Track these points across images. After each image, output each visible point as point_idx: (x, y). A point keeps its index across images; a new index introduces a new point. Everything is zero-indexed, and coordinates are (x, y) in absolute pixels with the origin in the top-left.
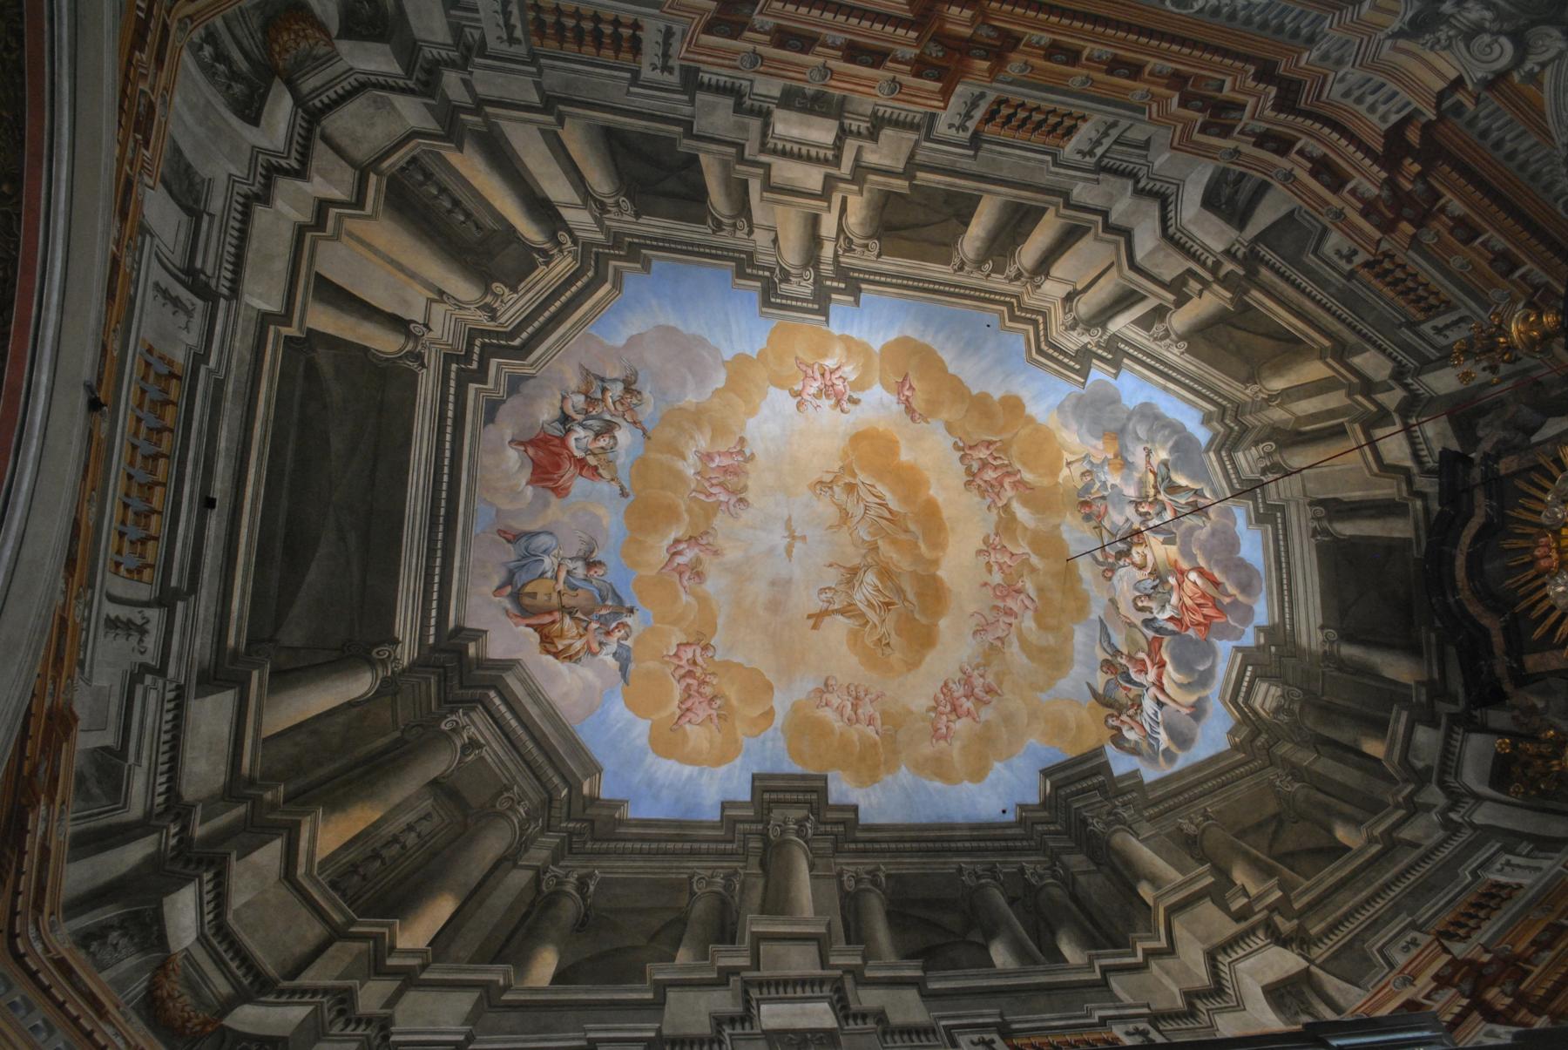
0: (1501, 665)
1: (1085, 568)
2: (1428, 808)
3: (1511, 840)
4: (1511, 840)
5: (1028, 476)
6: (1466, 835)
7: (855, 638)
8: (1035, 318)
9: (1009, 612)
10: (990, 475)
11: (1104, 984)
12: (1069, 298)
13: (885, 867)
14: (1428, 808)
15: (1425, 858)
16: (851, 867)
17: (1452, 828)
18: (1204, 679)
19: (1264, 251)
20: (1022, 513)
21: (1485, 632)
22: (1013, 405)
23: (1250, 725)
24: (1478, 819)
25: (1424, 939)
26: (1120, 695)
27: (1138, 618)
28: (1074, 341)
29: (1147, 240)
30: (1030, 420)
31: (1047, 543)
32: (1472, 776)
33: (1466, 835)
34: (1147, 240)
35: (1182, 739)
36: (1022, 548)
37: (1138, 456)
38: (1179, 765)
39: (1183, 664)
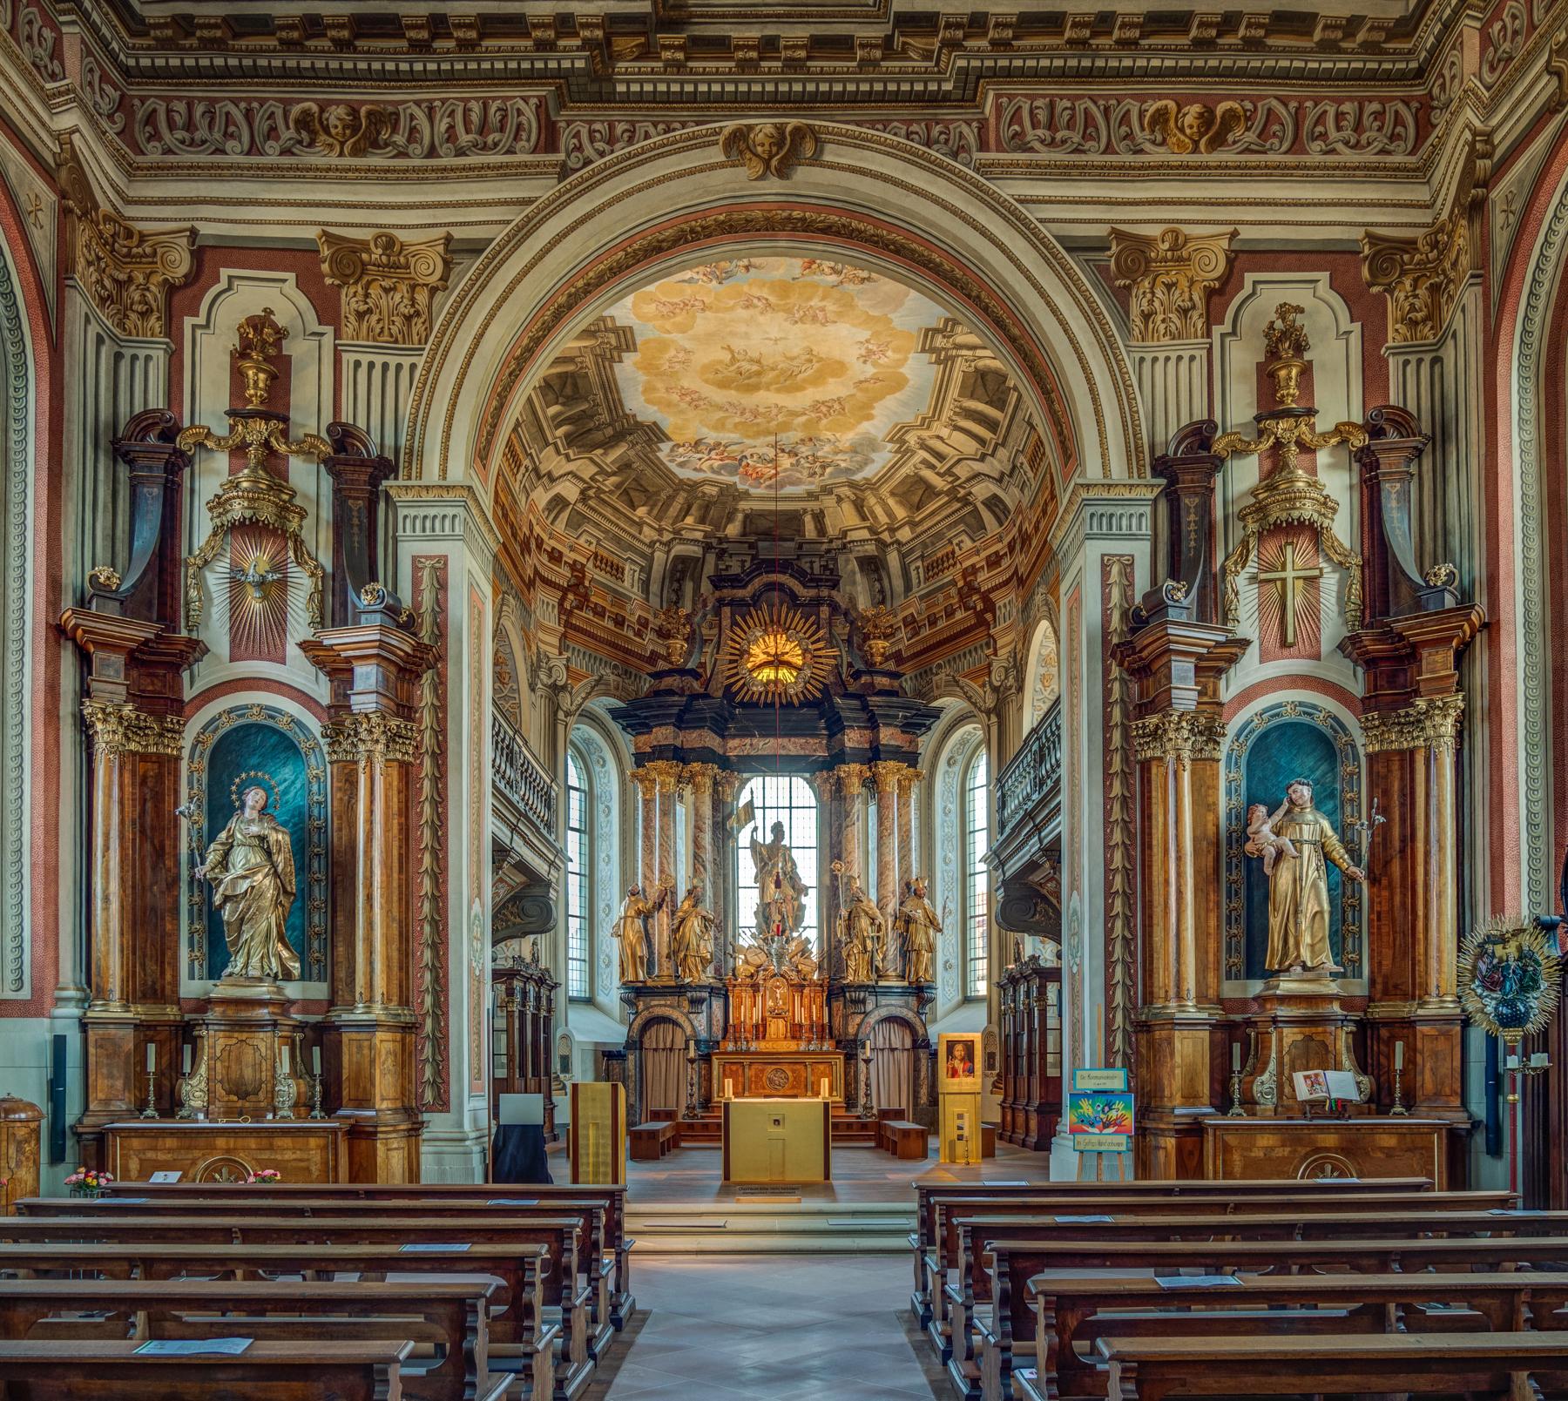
0: (727, 593)
1: (771, 439)
2: (661, 535)
3: (647, 570)
4: (647, 570)
5: (824, 421)
6: (648, 551)
7: (721, 362)
8: (926, 423)
9: (742, 414)
10: (824, 409)
11: (547, 444)
12: (939, 437)
13: (592, 372)
14: (661, 535)
15: (634, 537)
16: (589, 360)
17: (652, 544)
18: (714, 471)
19: (970, 508)
20: (803, 418)
21: (744, 587)
22: (869, 417)
23: (693, 487)
24: (657, 554)
25: (592, 547)
26: (702, 447)
27: (747, 453)
28: (912, 439)
29: (978, 467)
30: (859, 423)
31: (785, 427)
32: (678, 549)
33: (648, 551)
34: (978, 467)
35: (681, 465)
36: (780, 418)
37: (840, 457)
38: (670, 465)
39: (723, 467)
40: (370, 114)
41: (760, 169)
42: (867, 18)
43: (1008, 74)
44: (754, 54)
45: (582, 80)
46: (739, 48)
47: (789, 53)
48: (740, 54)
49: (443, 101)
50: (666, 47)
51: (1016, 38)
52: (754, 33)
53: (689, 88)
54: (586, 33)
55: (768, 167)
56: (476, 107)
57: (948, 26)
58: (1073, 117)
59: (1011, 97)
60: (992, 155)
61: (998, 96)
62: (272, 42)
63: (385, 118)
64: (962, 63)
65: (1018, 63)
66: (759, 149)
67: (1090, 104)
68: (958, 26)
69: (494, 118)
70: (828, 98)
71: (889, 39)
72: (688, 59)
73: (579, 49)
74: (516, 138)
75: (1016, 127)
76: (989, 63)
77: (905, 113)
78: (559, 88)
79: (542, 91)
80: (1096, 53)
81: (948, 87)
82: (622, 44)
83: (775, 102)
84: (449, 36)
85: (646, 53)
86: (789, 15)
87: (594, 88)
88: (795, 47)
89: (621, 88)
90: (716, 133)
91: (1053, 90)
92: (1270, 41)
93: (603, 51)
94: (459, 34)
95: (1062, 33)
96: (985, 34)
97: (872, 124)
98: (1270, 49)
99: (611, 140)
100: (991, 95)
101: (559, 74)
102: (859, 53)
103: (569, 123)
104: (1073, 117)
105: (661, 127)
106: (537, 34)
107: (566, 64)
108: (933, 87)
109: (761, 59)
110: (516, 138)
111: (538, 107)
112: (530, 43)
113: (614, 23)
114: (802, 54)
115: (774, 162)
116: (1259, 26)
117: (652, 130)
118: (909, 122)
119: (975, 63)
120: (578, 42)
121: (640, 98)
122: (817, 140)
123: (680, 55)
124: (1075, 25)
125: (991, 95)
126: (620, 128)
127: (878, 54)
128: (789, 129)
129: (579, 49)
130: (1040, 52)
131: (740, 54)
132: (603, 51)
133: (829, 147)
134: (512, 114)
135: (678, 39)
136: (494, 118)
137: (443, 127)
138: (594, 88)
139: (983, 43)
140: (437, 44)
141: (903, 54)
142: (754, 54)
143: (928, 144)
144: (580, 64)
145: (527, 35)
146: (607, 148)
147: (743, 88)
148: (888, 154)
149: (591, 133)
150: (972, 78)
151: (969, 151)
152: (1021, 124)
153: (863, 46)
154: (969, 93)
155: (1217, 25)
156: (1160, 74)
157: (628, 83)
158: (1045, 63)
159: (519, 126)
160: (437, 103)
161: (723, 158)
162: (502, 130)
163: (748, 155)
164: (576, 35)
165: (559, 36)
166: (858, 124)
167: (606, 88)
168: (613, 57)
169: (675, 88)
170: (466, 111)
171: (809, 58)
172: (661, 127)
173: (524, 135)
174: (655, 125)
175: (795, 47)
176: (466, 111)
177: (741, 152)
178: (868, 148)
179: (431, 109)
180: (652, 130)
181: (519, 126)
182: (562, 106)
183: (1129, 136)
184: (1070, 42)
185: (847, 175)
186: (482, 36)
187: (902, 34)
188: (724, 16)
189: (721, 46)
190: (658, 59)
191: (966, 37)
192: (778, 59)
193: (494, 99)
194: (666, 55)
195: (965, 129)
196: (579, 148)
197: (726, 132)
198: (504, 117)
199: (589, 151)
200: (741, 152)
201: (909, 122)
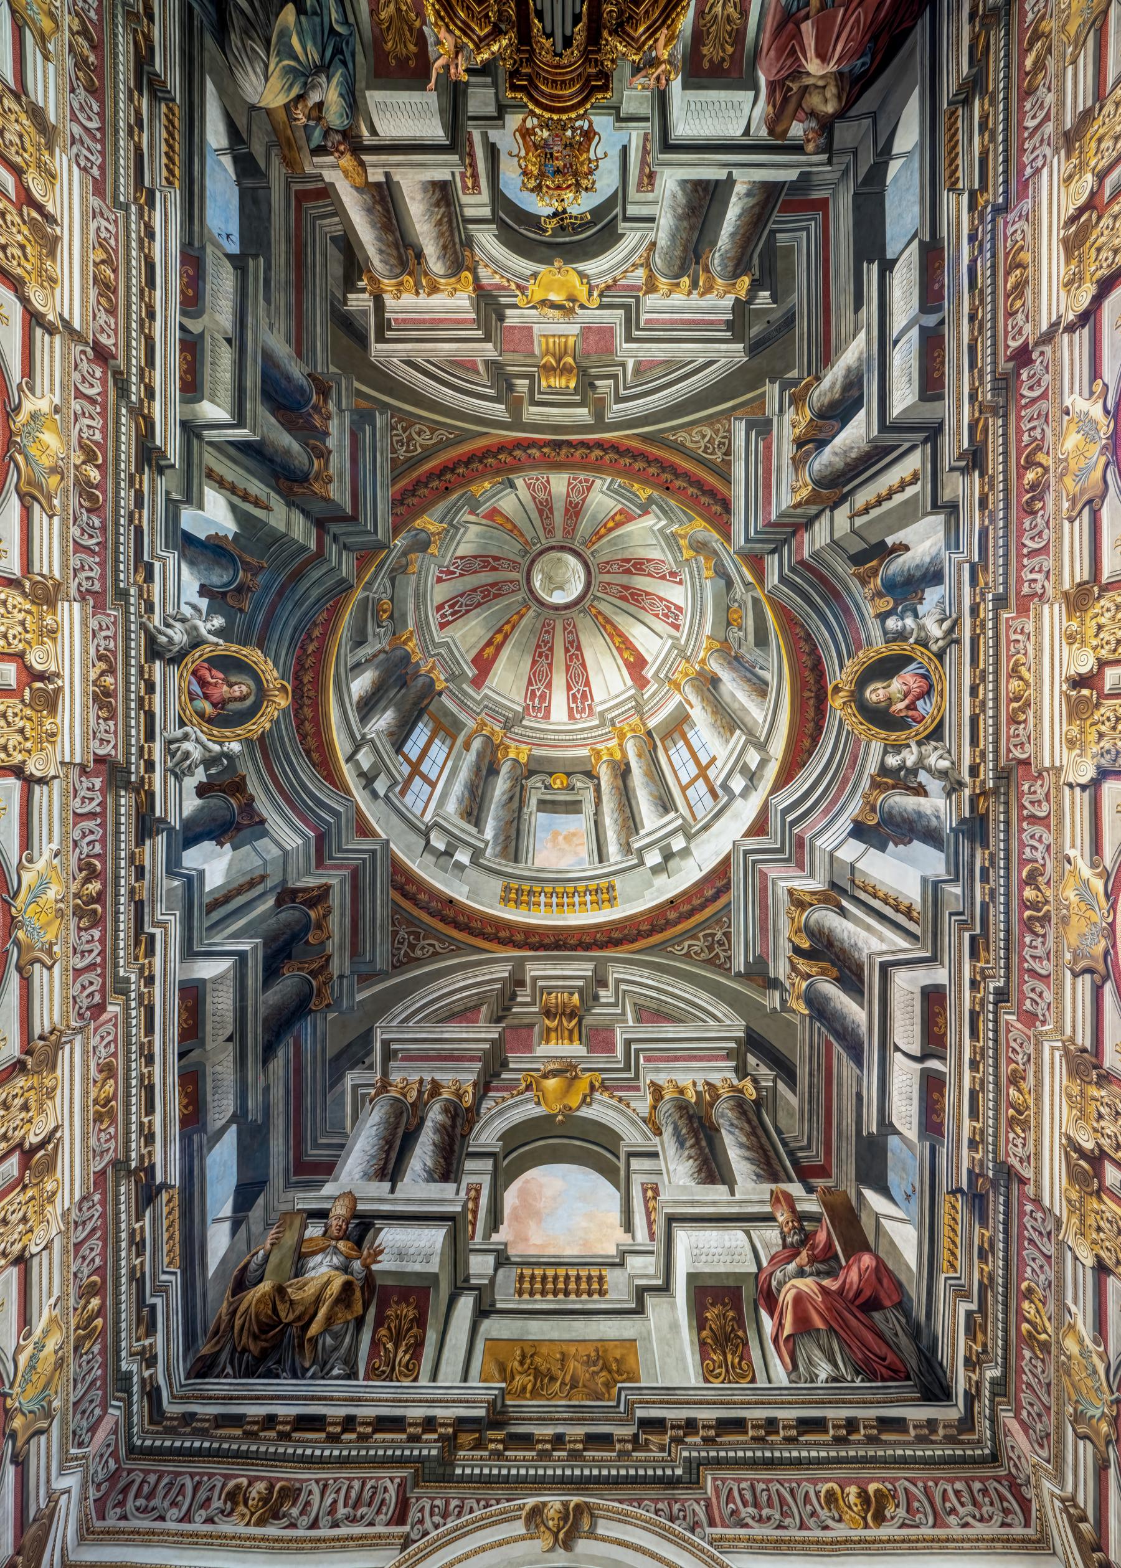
40: (282, 1489)
41: (551, 1541)
42: (622, 1422)
43: (718, 1463)
44: (548, 1446)
45: (433, 1465)
46: (539, 1441)
47: (572, 1446)
48: (540, 1446)
49: (335, 1480)
50: (492, 1441)
51: (717, 1435)
52: (549, 1431)
53: (504, 1472)
54: (442, 1430)
55: (556, 1535)
56: (356, 1485)
57: (673, 1427)
58: (769, 1497)
59: (724, 1480)
60: (719, 1531)
61: (715, 1480)
62: (238, 1432)
63: (291, 1493)
64: (685, 1454)
65: (722, 1454)
66: (551, 1523)
67: (778, 1486)
68: (679, 1427)
69: (366, 1495)
70: (597, 1480)
71: (636, 1436)
72: (505, 1449)
73: (436, 1441)
74: (378, 1512)
75: (731, 1505)
76: (703, 1454)
77: (653, 1493)
78: (417, 1470)
79: (404, 1473)
80: (772, 1447)
81: (679, 1472)
82: (466, 1438)
83: (562, 1483)
84: (353, 1430)
85: (478, 1445)
86: (571, 1419)
87: (440, 1471)
88: (575, 1441)
89: (458, 1471)
90: (521, 1508)
91: (751, 1475)
92: (884, 1437)
93: (450, 1443)
94: (361, 1429)
95: (746, 1433)
96: (697, 1433)
97: (630, 1502)
98: (885, 1442)
99: (445, 1515)
100: (709, 1478)
101: (420, 1460)
102: (618, 1446)
103: (418, 1499)
104: (769, 1497)
105: (482, 1503)
106: (411, 1430)
107: (425, 1452)
108: (669, 1472)
109: (554, 1450)
110: (378, 1512)
111: (399, 1485)
112: (404, 1436)
113: (461, 1423)
114: (580, 1446)
115: (561, 1535)
116: (872, 1427)
117: (475, 1506)
118: (656, 1501)
119: (695, 1454)
120: (435, 1436)
121: (471, 1479)
122: (592, 1516)
123: (500, 1447)
124: (753, 1427)
125: (709, 1478)
126: (454, 1503)
127: (630, 1447)
128: (572, 1505)
129: (436, 1441)
130: (735, 1447)
131: (540, 1446)
132: (450, 1443)
133: (601, 1522)
134: (380, 1490)
135: (499, 1435)
136: (366, 1495)
137: (330, 1501)
138: (440, 1471)
139: (698, 1439)
140: (345, 1437)
141: (645, 1447)
142: (548, 1446)
143: (672, 1520)
144: (434, 1452)
145: (404, 1431)
146: (442, 1521)
147: (541, 1472)
148: (644, 1528)
149: (432, 1507)
150: (694, 1465)
151: (702, 1527)
152: (735, 1503)
153: (619, 1441)
154: (694, 1477)
155: (844, 1427)
156: (819, 1462)
157: (464, 1467)
158: (740, 1454)
159: (383, 1500)
160: (331, 1482)
161: (524, 1531)
162: (370, 1505)
163: (543, 1529)
164: (435, 1431)
165: (424, 1432)
166: (621, 1502)
167: (448, 1471)
168: (457, 1447)
169: (495, 1471)
170: (350, 1487)
171: (585, 1449)
172: (482, 1503)
173: (384, 1509)
174: (478, 1502)
175: (575, 1441)
176: (350, 1487)
177: (537, 1526)
178: (625, 1522)
179: (325, 1486)
180: (475, 1506)
181: (383, 1500)
182: (416, 1485)
183: (813, 1514)
184: (753, 1438)
185: (615, 1547)
186: (375, 1431)
187: (644, 1433)
188: (530, 1419)
189: (526, 1441)
190: (486, 1449)
191: (685, 1435)
192: (564, 1450)
193: (371, 1478)
194: (492, 1446)
195: (696, 1507)
196: (421, 1522)
197: (528, 1507)
198: (374, 1493)
199: (428, 1524)
200: (537, 1526)
201: (656, 1501)
